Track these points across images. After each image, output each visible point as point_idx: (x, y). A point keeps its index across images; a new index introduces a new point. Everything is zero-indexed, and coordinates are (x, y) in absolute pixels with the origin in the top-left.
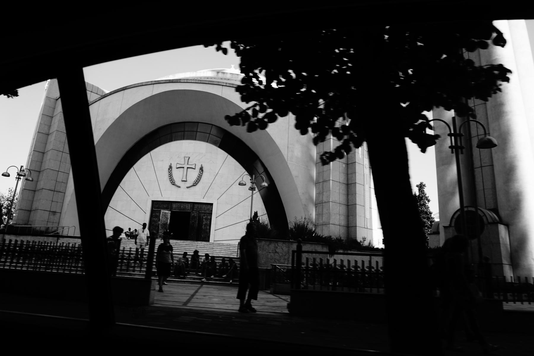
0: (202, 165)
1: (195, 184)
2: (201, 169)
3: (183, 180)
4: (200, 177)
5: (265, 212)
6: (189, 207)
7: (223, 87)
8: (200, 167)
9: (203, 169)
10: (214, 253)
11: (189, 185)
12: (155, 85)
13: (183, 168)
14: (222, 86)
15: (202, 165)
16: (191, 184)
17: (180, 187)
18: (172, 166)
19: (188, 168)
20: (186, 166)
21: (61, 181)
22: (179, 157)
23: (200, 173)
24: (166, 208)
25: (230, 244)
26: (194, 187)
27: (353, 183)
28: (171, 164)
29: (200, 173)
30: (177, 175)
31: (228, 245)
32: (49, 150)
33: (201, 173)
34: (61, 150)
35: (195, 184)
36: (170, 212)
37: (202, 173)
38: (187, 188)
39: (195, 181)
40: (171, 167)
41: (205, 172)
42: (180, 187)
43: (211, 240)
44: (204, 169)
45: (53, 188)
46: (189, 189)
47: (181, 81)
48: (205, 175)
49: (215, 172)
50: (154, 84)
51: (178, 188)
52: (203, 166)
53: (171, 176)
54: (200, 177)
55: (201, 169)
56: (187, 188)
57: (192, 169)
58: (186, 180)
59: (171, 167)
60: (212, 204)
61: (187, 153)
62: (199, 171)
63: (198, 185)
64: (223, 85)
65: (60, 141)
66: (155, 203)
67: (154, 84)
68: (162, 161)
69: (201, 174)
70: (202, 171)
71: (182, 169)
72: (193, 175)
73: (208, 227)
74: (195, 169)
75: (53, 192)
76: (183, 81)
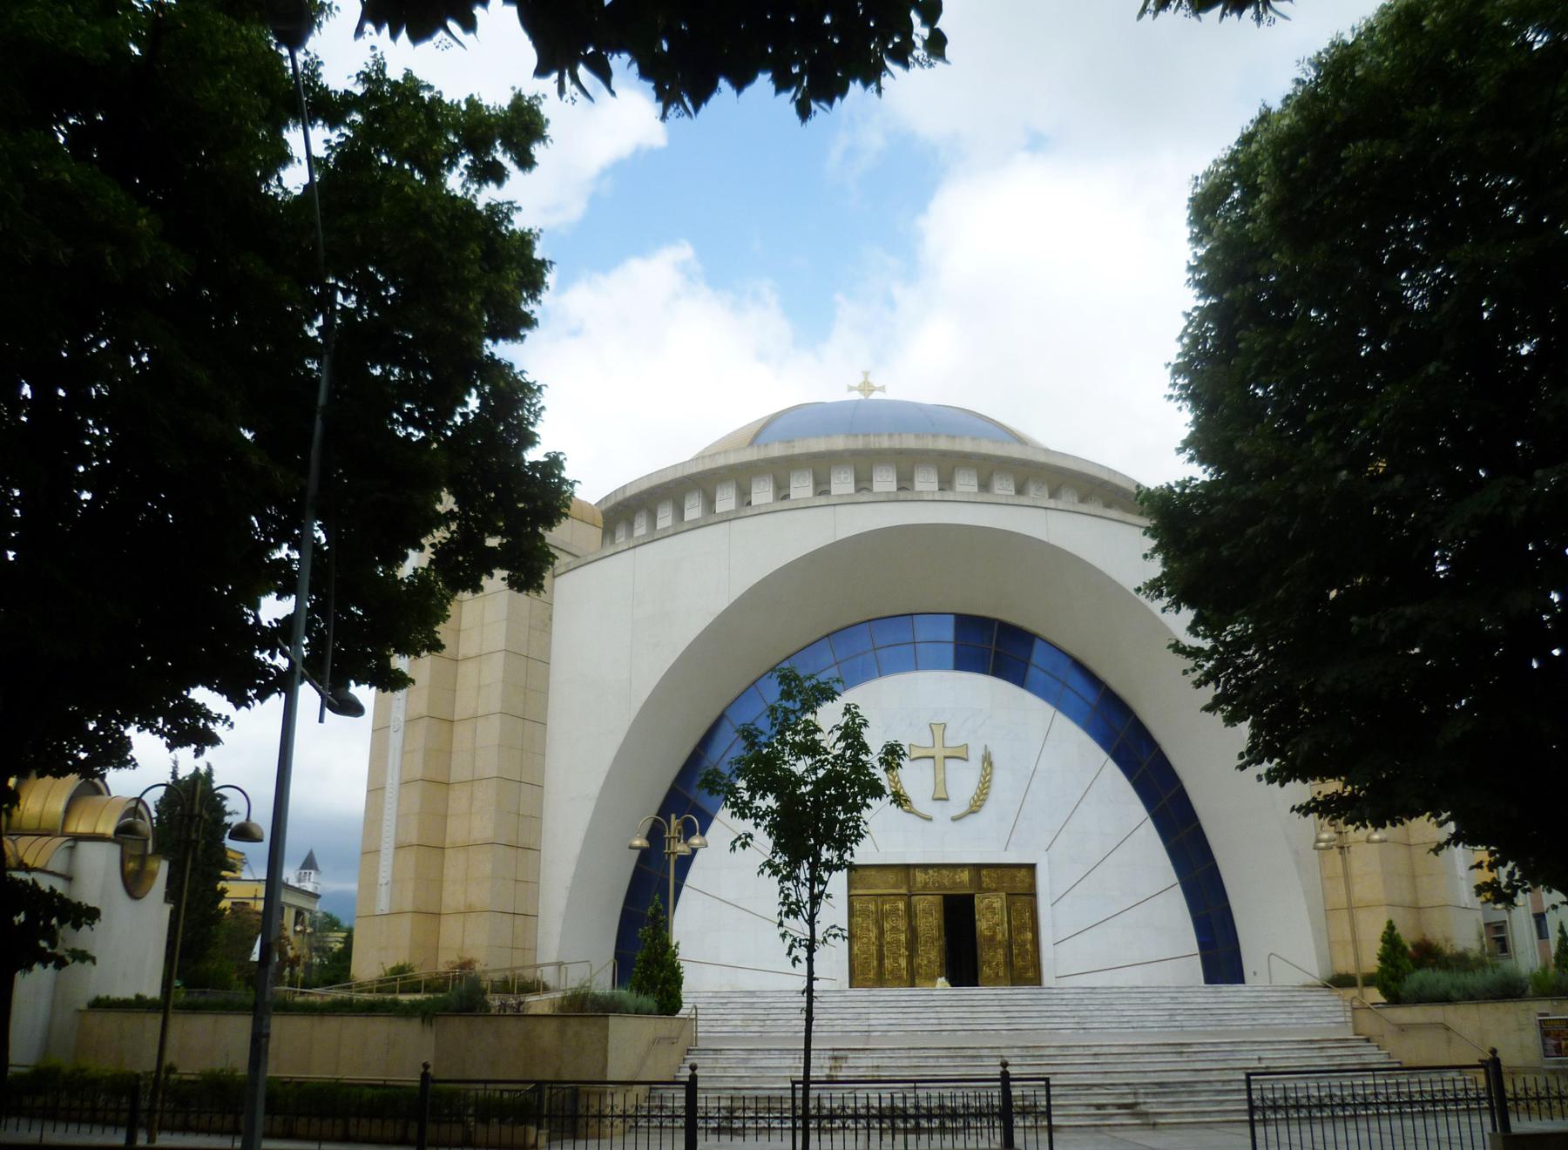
0: (986, 746)
1: (975, 807)
2: (987, 760)
3: (937, 796)
4: (986, 785)
5: (1176, 880)
6: (965, 876)
7: (1049, 511)
8: (981, 752)
9: (992, 759)
11: (957, 813)
12: (837, 507)
13: (933, 757)
14: (1043, 511)
15: (986, 746)
16: (965, 808)
17: (930, 819)
19: (946, 757)
20: (939, 753)
23: (985, 771)
25: (1138, 987)
26: (973, 816)
29: (985, 771)
31: (1135, 990)
32: (480, 712)
35: (975, 807)
37: (991, 773)
38: (954, 819)
39: (973, 798)
42: (930, 819)
43: (1048, 978)
44: (995, 759)
47: (926, 498)
48: (1000, 778)
50: (835, 505)
51: (923, 821)
52: (990, 749)
53: (896, 784)
54: (986, 785)
55: (987, 760)
56: (954, 819)
57: (962, 761)
58: (944, 796)
60: (1031, 868)
62: (980, 765)
63: (983, 809)
67: (835, 505)
69: (987, 775)
70: (991, 764)
72: (964, 780)
73: (1029, 935)
74: (966, 760)
75: (514, 850)
76: (930, 498)
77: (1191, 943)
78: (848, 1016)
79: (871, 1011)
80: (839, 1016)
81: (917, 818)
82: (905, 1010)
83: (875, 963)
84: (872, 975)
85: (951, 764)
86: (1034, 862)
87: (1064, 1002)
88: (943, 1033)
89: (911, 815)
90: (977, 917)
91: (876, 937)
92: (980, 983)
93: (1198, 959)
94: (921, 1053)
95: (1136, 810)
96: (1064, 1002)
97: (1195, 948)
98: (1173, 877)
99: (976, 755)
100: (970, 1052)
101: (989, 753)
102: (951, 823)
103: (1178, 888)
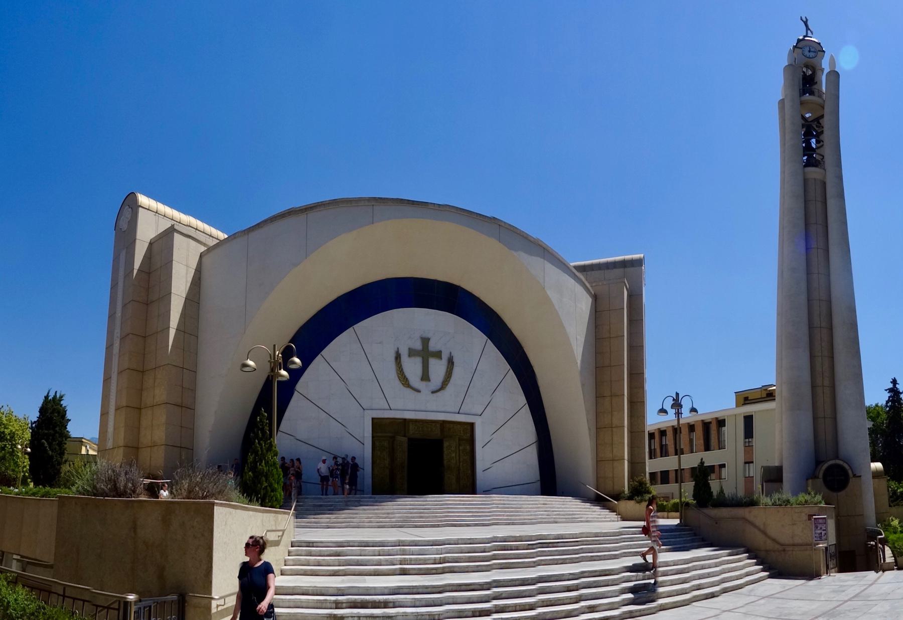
0: (451, 353)
11: (435, 388)
17: (418, 391)
18: (400, 351)
28: (398, 348)
30: (413, 368)
36: (406, 438)
38: (433, 392)
40: (398, 357)
41: (456, 366)
42: (418, 391)
44: (455, 360)
46: (435, 395)
48: (457, 371)
59: (398, 357)
68: (380, 343)
70: (453, 363)
81: (413, 391)
86: (474, 422)
89: (408, 390)
99: (445, 356)
101: (452, 357)
102: (431, 394)
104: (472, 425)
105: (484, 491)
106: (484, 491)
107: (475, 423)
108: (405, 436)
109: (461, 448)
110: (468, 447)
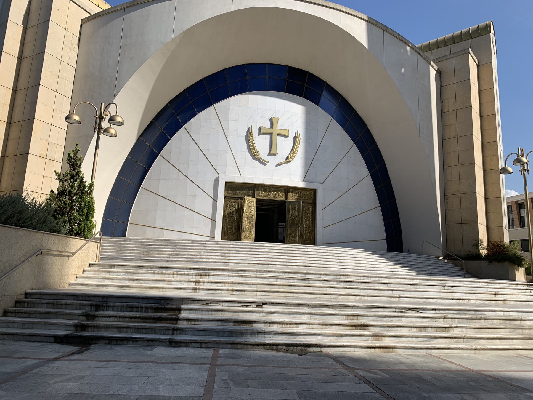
10: (231, 255)
20: (275, 132)
21: (56, 143)
22: (262, 117)
24: (248, 195)
27: (492, 168)
29: (297, 143)
33: (298, 143)
34: (54, 88)
36: (255, 200)
45: (44, 154)
49: (317, 143)
61: (275, 112)
64: (341, 11)
65: (51, 72)
66: (230, 186)
68: (236, 120)
71: (269, 137)
75: (44, 160)
77: (382, 235)
78: (218, 254)
79: (231, 252)
80: (213, 254)
82: (249, 253)
83: (235, 231)
84: (233, 236)
85: (279, 138)
87: (331, 254)
88: (269, 266)
90: (287, 212)
91: (236, 218)
92: (285, 242)
93: (385, 242)
94: (264, 274)
95: (364, 170)
96: (331, 254)
97: (384, 237)
98: (378, 204)
100: (299, 276)
103: (379, 208)
104: (315, 191)
105: (322, 244)
106: (322, 244)
107: (317, 189)
108: (254, 197)
109: (304, 209)
110: (311, 209)
